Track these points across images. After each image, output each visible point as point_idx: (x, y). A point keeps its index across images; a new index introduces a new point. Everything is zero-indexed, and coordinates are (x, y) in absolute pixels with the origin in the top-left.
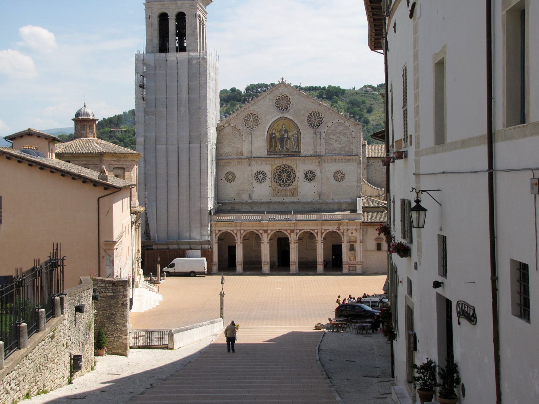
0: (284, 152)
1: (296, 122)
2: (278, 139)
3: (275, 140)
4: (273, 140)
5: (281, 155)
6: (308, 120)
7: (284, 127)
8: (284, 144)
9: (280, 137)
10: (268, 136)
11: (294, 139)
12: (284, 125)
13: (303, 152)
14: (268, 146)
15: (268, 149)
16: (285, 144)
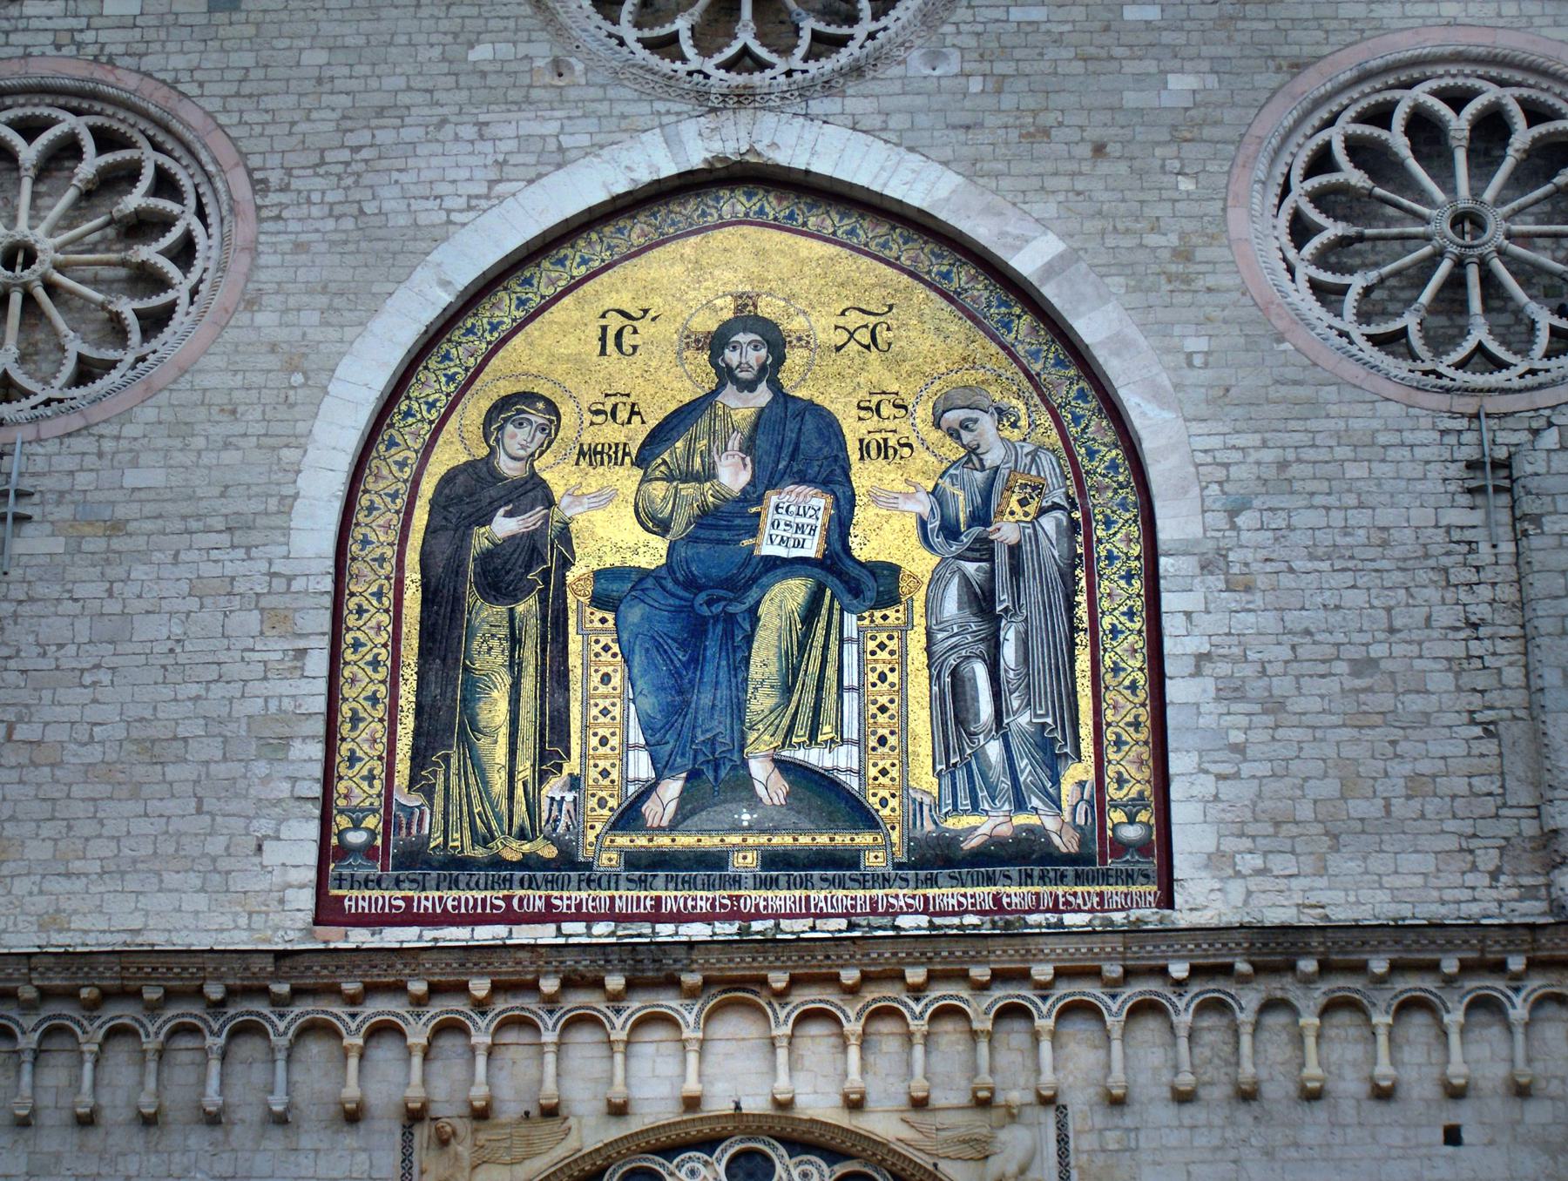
0: (746, 863)
1: (1026, 263)
2: (599, 601)
3: (527, 607)
4: (487, 615)
5: (679, 918)
6: (1301, 230)
7: (747, 354)
8: (738, 708)
9: (651, 552)
10: (376, 530)
11: (981, 601)
12: (747, 319)
13: (1217, 861)
14: (364, 740)
15: (356, 789)
16: (761, 702)
